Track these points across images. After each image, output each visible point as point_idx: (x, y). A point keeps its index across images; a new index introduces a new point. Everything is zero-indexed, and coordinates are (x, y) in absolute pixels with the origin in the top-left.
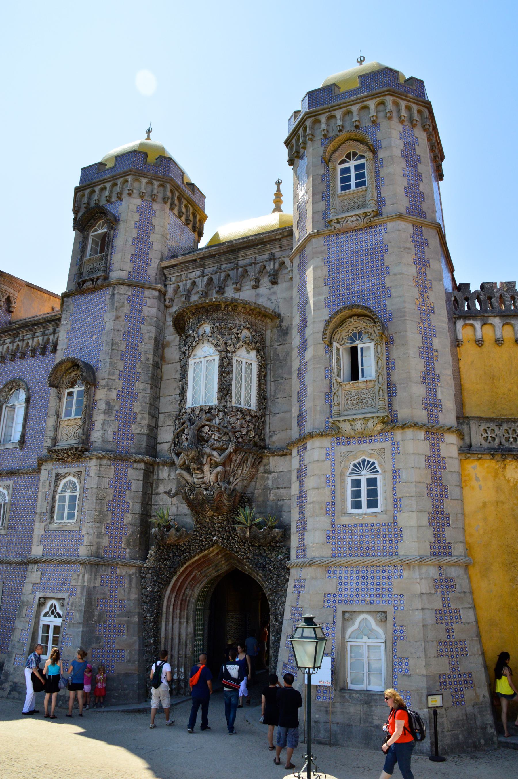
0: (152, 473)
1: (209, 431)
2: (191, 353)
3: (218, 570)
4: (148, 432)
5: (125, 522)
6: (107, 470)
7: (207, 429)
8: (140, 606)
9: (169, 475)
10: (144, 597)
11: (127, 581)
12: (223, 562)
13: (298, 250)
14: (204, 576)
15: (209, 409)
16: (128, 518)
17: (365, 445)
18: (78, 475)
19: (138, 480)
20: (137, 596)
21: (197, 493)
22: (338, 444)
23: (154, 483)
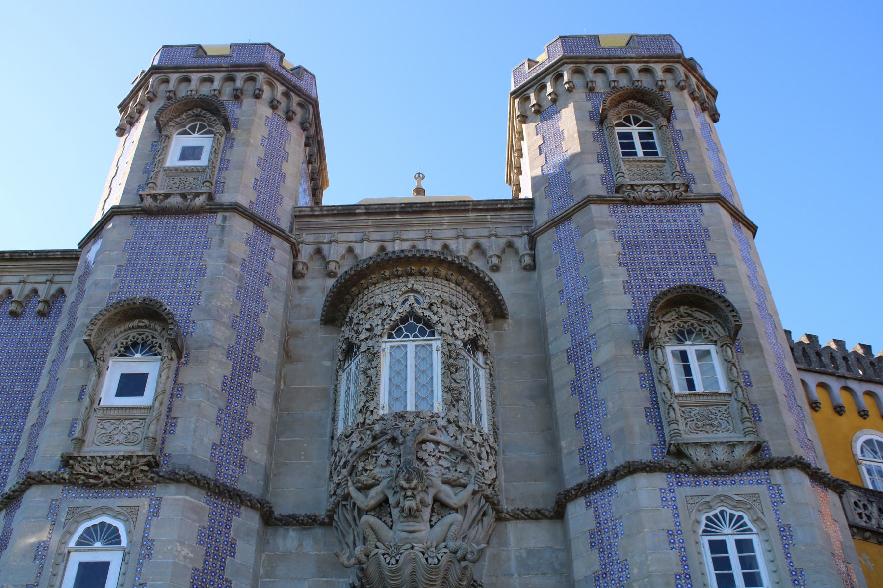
7: (430, 447)
17: (725, 487)
18: (129, 515)
22: (680, 484)
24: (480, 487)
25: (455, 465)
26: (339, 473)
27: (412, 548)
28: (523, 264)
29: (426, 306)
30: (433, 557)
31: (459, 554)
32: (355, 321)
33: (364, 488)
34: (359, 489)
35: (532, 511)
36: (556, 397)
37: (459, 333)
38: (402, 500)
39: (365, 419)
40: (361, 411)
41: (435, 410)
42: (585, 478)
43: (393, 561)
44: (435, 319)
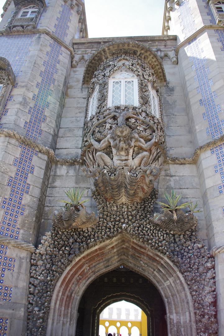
0: (50, 170)
1: (135, 123)
2: (112, 74)
3: (108, 266)
4: (53, 134)
5: (23, 202)
6: (15, 149)
7: (133, 120)
8: (27, 298)
9: (68, 172)
10: (32, 287)
11: (17, 264)
12: (116, 257)
13: (188, 40)
14: (92, 272)
15: (134, 108)
16: (27, 199)
19: (41, 168)
20: (25, 284)
21: (119, 174)
23: (51, 178)
24: (158, 142)
25: (145, 130)
26: (86, 136)
27: (123, 168)
28: (172, 61)
29: (130, 64)
30: (134, 174)
31: (148, 172)
32: (97, 74)
33: (99, 141)
34: (96, 141)
35: (181, 159)
36: (192, 108)
37: (146, 77)
38: (118, 143)
39: (100, 111)
40: (98, 108)
41: (135, 105)
42: (210, 140)
43: (113, 175)
44: (135, 69)
